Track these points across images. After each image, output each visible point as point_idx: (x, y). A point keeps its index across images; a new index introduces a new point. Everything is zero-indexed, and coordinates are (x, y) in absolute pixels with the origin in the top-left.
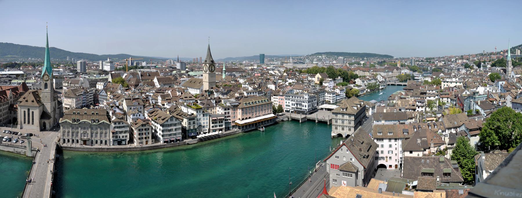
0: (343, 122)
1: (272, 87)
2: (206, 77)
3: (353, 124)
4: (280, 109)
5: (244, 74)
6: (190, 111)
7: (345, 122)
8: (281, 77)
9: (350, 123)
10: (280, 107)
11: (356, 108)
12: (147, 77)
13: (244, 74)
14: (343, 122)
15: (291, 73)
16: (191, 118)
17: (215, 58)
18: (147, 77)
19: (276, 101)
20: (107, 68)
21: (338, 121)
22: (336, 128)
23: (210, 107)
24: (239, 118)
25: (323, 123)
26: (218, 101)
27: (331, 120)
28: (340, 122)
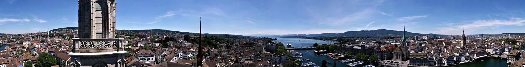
1: (486, 46)
2: (462, 42)
4: (489, 53)
5: (475, 40)
6: (457, 54)
8: (489, 42)
10: (489, 53)
12: (441, 42)
13: (475, 40)
15: (493, 41)
16: (457, 57)
17: (466, 35)
18: (441, 42)
19: (488, 51)
20: (426, 39)
23: (464, 53)
24: (475, 57)
26: (467, 51)
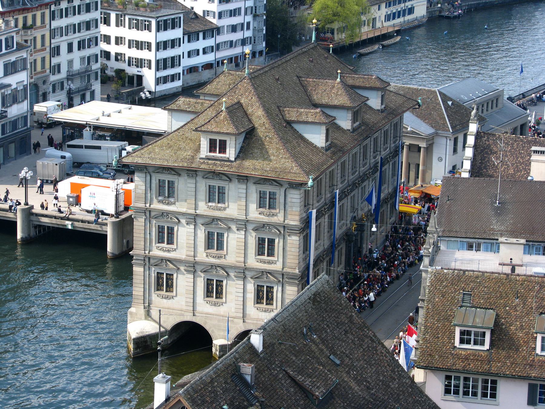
0: (215, 241)
3: (289, 254)
7: (234, 240)
9: (265, 247)
11: (318, 138)
14: (215, 241)
21: (184, 233)
22: (165, 283)
25: (72, 247)
27: (125, 227)
28: (188, 241)
